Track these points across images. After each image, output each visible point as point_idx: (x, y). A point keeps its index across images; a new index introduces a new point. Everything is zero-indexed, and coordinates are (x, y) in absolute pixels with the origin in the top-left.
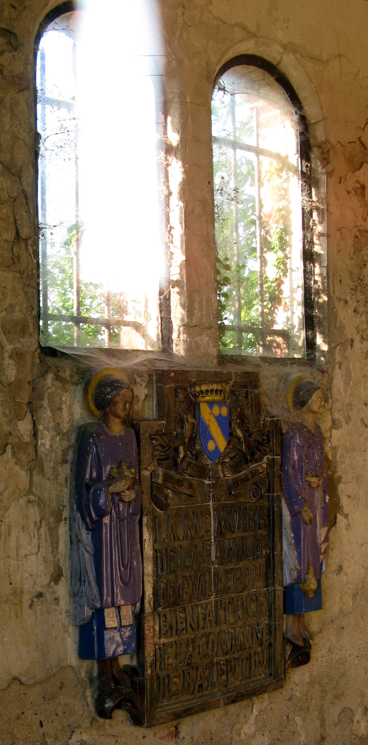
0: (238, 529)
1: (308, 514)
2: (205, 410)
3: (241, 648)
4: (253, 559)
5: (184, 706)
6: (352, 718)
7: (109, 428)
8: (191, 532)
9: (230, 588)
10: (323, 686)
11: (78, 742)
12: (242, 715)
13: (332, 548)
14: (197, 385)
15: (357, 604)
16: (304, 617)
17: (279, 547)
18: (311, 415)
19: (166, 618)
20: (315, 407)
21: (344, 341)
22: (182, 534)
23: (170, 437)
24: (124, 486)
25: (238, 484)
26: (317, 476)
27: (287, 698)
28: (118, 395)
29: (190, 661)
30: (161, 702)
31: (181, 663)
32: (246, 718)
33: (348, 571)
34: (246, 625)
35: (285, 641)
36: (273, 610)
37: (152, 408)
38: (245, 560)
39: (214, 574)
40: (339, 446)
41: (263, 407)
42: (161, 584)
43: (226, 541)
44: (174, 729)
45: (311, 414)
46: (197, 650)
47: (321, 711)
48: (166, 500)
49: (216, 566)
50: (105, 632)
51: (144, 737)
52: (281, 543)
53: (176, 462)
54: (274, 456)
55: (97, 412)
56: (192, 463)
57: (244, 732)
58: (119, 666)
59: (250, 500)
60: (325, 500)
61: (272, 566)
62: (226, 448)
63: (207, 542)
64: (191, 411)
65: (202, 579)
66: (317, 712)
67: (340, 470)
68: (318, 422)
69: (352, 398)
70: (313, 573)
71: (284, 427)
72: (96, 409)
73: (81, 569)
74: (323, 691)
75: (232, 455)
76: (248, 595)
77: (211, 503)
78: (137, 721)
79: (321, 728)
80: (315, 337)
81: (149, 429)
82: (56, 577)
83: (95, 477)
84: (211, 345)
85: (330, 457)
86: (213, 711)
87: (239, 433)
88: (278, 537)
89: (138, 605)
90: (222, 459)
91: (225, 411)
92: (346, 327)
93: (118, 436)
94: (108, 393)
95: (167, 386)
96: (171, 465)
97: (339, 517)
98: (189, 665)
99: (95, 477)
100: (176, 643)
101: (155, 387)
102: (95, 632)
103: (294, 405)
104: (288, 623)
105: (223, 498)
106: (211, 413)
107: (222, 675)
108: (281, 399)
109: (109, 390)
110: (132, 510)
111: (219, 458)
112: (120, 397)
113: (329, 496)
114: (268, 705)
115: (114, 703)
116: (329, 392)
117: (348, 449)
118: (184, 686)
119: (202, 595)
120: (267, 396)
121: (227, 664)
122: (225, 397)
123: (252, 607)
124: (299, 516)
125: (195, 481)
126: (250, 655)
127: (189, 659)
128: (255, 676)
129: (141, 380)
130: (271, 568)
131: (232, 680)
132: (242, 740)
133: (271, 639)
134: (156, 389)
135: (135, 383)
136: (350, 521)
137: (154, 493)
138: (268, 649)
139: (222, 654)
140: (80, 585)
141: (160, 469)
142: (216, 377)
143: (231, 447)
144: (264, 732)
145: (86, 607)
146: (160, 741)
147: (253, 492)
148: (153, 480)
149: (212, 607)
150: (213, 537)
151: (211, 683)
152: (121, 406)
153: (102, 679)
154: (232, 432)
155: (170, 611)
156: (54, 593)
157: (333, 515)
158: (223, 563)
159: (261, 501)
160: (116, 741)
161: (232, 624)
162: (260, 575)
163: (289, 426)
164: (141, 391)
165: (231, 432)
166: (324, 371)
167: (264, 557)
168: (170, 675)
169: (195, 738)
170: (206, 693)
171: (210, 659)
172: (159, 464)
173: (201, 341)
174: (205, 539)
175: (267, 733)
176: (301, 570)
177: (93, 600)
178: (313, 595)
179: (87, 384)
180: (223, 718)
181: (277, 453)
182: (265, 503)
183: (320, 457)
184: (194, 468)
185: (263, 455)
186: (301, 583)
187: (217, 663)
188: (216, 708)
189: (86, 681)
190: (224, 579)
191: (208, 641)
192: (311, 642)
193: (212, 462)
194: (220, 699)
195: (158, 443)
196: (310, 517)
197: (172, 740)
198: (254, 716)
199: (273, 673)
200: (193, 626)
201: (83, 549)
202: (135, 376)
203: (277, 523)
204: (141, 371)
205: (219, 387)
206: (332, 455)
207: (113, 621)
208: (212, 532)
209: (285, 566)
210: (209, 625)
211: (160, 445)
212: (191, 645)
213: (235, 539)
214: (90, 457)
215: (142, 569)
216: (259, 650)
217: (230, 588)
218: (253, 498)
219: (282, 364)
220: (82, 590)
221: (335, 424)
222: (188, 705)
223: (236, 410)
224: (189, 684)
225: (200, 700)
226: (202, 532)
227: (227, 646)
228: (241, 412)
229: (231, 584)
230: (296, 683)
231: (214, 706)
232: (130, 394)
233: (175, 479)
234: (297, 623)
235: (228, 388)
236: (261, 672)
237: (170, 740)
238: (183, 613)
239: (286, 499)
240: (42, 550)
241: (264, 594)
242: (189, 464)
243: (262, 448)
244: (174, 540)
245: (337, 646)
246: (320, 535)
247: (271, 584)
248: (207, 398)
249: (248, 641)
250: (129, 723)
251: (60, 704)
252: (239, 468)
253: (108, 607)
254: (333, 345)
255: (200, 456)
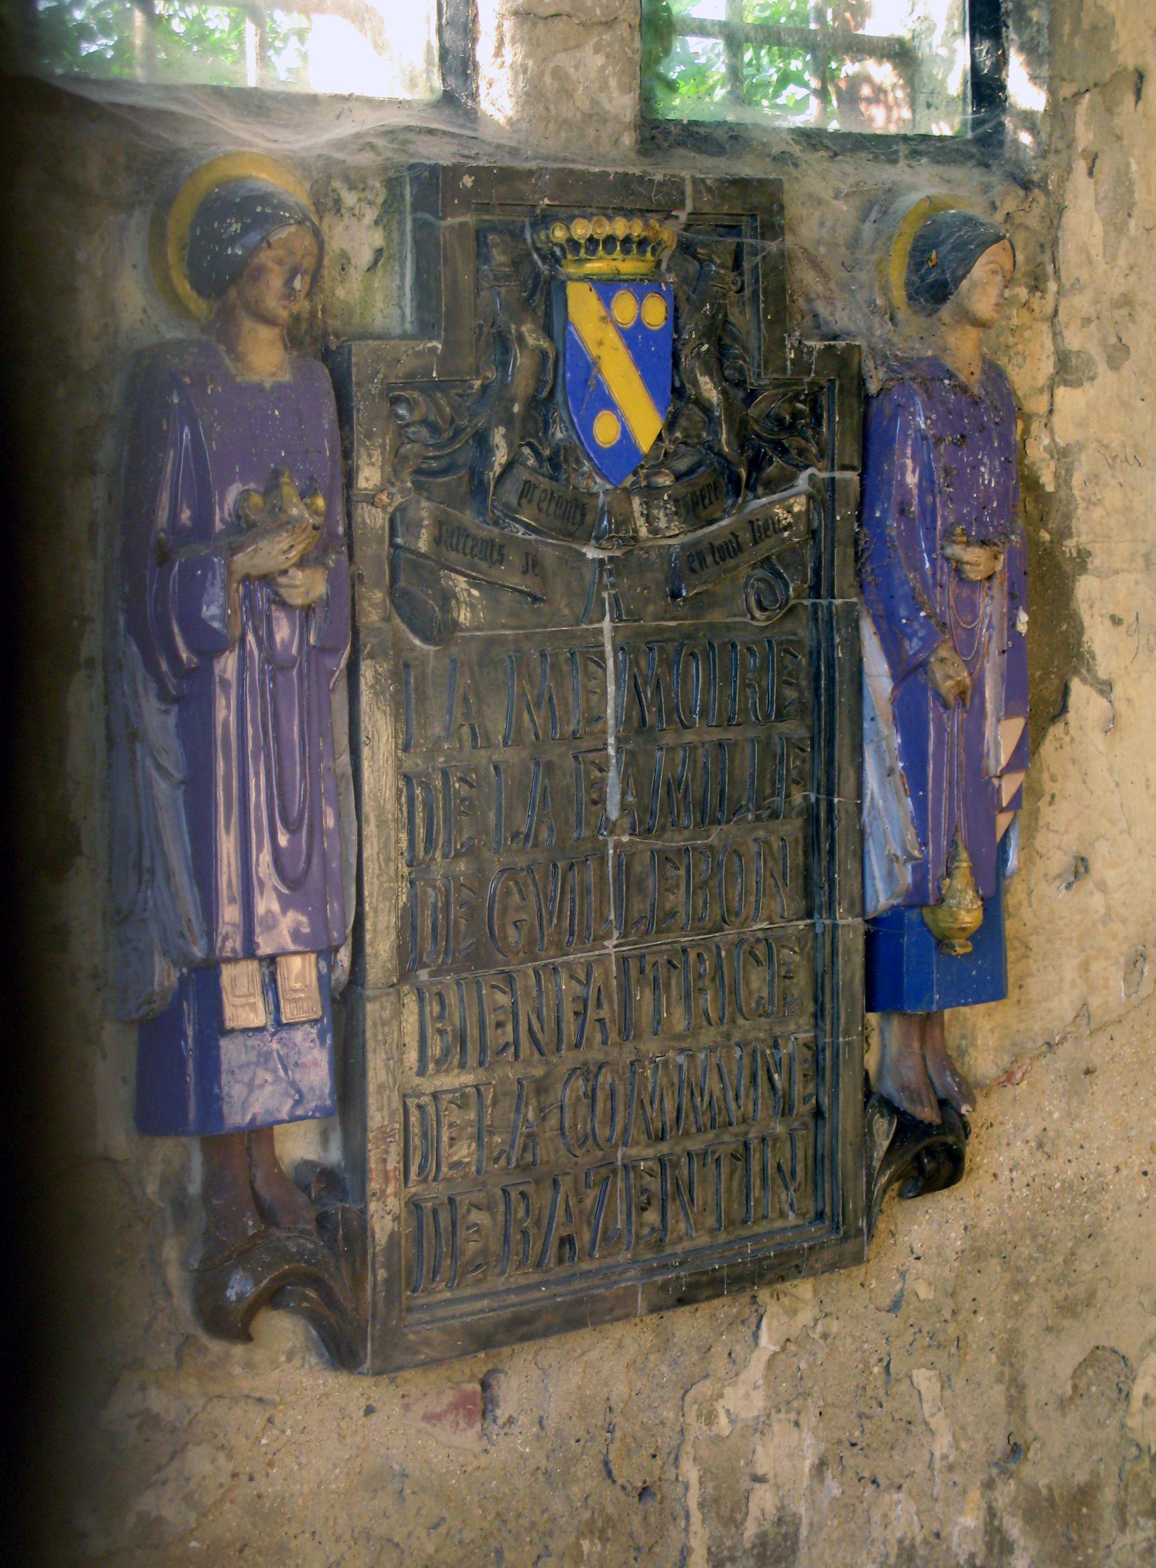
0: (704, 713)
1: (951, 672)
2: (583, 306)
3: (713, 1119)
4: (758, 818)
5: (506, 1307)
6: (1124, 1387)
7: (239, 358)
8: (533, 721)
9: (673, 914)
10: (1019, 1269)
12: (719, 1350)
13: (1053, 796)
14: (557, 219)
15: (1144, 991)
16: (942, 1024)
17: (852, 781)
18: (973, 333)
19: (442, 1004)
20: (983, 305)
21: (1108, 76)
22: (502, 726)
23: (460, 396)
24: (284, 552)
25: (702, 562)
26: (984, 543)
27: (887, 1302)
28: (264, 245)
29: (529, 1158)
30: (430, 1292)
31: (496, 1160)
32: (734, 1362)
33: (1111, 876)
34: (732, 1042)
35: (873, 1101)
36: (828, 997)
37: (401, 297)
38: (728, 822)
39: (618, 865)
40: (1081, 446)
41: (801, 303)
42: (425, 893)
43: (658, 754)
44: (478, 1388)
45: (968, 327)
46: (553, 1121)
47: (1010, 1354)
48: (445, 607)
49: (625, 839)
50: (224, 1043)
51: (369, 1411)
52: (860, 768)
53: (481, 481)
54: (832, 470)
55: (198, 305)
56: (535, 487)
57: (728, 1412)
58: (275, 1162)
59: (748, 619)
60: (1014, 625)
61: (825, 846)
62: (660, 437)
63: (591, 756)
64: (534, 310)
65: (575, 876)
66: (993, 1357)
67: (1084, 528)
68: (1002, 361)
69: (1132, 278)
70: (967, 872)
71: (873, 373)
72: (195, 295)
73: (140, 832)
74: (1017, 1286)
75: (682, 465)
76: (741, 942)
77: (607, 624)
78: (341, 1350)
79: (1009, 1414)
80: (1001, 63)
81: (382, 367)
83: (188, 523)
84: (613, 82)
85: (1048, 482)
86: (618, 1330)
87: (709, 389)
88: (846, 750)
89: (344, 957)
90: (647, 476)
91: (655, 313)
92: (1118, 25)
93: (268, 385)
94: (234, 239)
95: (449, 221)
96: (464, 489)
97: (1079, 690)
98: (524, 1168)
99: (188, 523)
100: (478, 1091)
101: (409, 226)
102: (190, 1040)
103: (910, 298)
104: (883, 1046)
105: (651, 608)
106: (608, 319)
107: (644, 1209)
108: (863, 276)
109: (236, 227)
110: (318, 637)
111: (635, 473)
112: (272, 253)
113: (1027, 612)
114: (816, 1321)
115: (257, 1282)
116: (1047, 257)
117: (1114, 458)
118: (506, 1240)
119: (572, 934)
120: (815, 264)
121: (663, 1173)
122: (658, 264)
123: (755, 985)
124: (921, 678)
125: (550, 550)
126: (746, 1145)
127: (525, 1148)
128: (765, 1217)
129: (360, 200)
130: (824, 855)
131: (682, 1226)
132: (718, 1436)
133: (821, 1095)
134: (414, 231)
135: (339, 210)
136: (1121, 706)
137: (402, 583)
138: (812, 1130)
139: (643, 1138)
140: (140, 883)
141: (424, 504)
142: (625, 195)
143: (678, 434)
144: (799, 1413)
145: (157, 959)
146: (423, 1425)
147: (758, 593)
148: (399, 541)
149: (607, 973)
150: (611, 740)
151: (605, 1233)
152: (276, 281)
153: (215, 1202)
154: (683, 385)
155: (458, 984)
157: (1056, 682)
158: (649, 831)
159: (788, 625)
160: (270, 1420)
161: (681, 1037)
162: (784, 874)
163: (890, 369)
164: (358, 236)
165: (677, 384)
166: (1032, 182)
167: (799, 814)
168: (458, 1199)
169: (551, 1423)
170: (585, 1266)
171: (600, 1154)
172: (418, 486)
173: (576, 67)
174: (585, 745)
175: (810, 1419)
176: (926, 861)
177: (182, 935)
178: (969, 949)
179: (165, 205)
180: (652, 1357)
181: (847, 462)
182: (804, 632)
183: (998, 476)
184: (544, 505)
185: (797, 466)
186: (926, 905)
187: (625, 1166)
188: (618, 1319)
189: (162, 1210)
190: (650, 883)
191: (594, 1090)
192: (964, 1109)
193: (609, 487)
194: (631, 1293)
195: (417, 416)
196: (958, 683)
197: (472, 1426)
198: (764, 1358)
199: (828, 1209)
200: (540, 1036)
201: (149, 762)
202: (336, 184)
203: (843, 700)
204: (358, 169)
205: (637, 229)
206: (1056, 475)
207: (253, 1007)
208: (611, 722)
209: (871, 846)
210: (598, 1037)
211: (424, 422)
212: (533, 1102)
213: (693, 748)
214: (172, 454)
215: (355, 838)
216: (779, 1129)
217: (673, 914)
218: (758, 614)
219: (876, 158)
220: (146, 902)
221: (1066, 368)
222: (521, 1304)
223: (698, 309)
224: (524, 1233)
225: (563, 1289)
226: (574, 721)
227: (662, 1110)
228: (714, 316)
229: (676, 900)
230: (918, 1251)
231: (612, 1310)
232: (308, 241)
233: (474, 538)
234: (916, 1045)
235: (668, 234)
236: (786, 1207)
237: (462, 1425)
238: (504, 992)
239: (876, 620)
241: (799, 940)
242: (527, 490)
243: (792, 443)
244: (475, 747)
245: (1068, 1132)
246: (997, 744)
247: (821, 906)
248: (595, 266)
249: (737, 1097)
250: (314, 1360)
252: (705, 508)
253: (233, 960)
254: (1067, 90)
255: (566, 460)
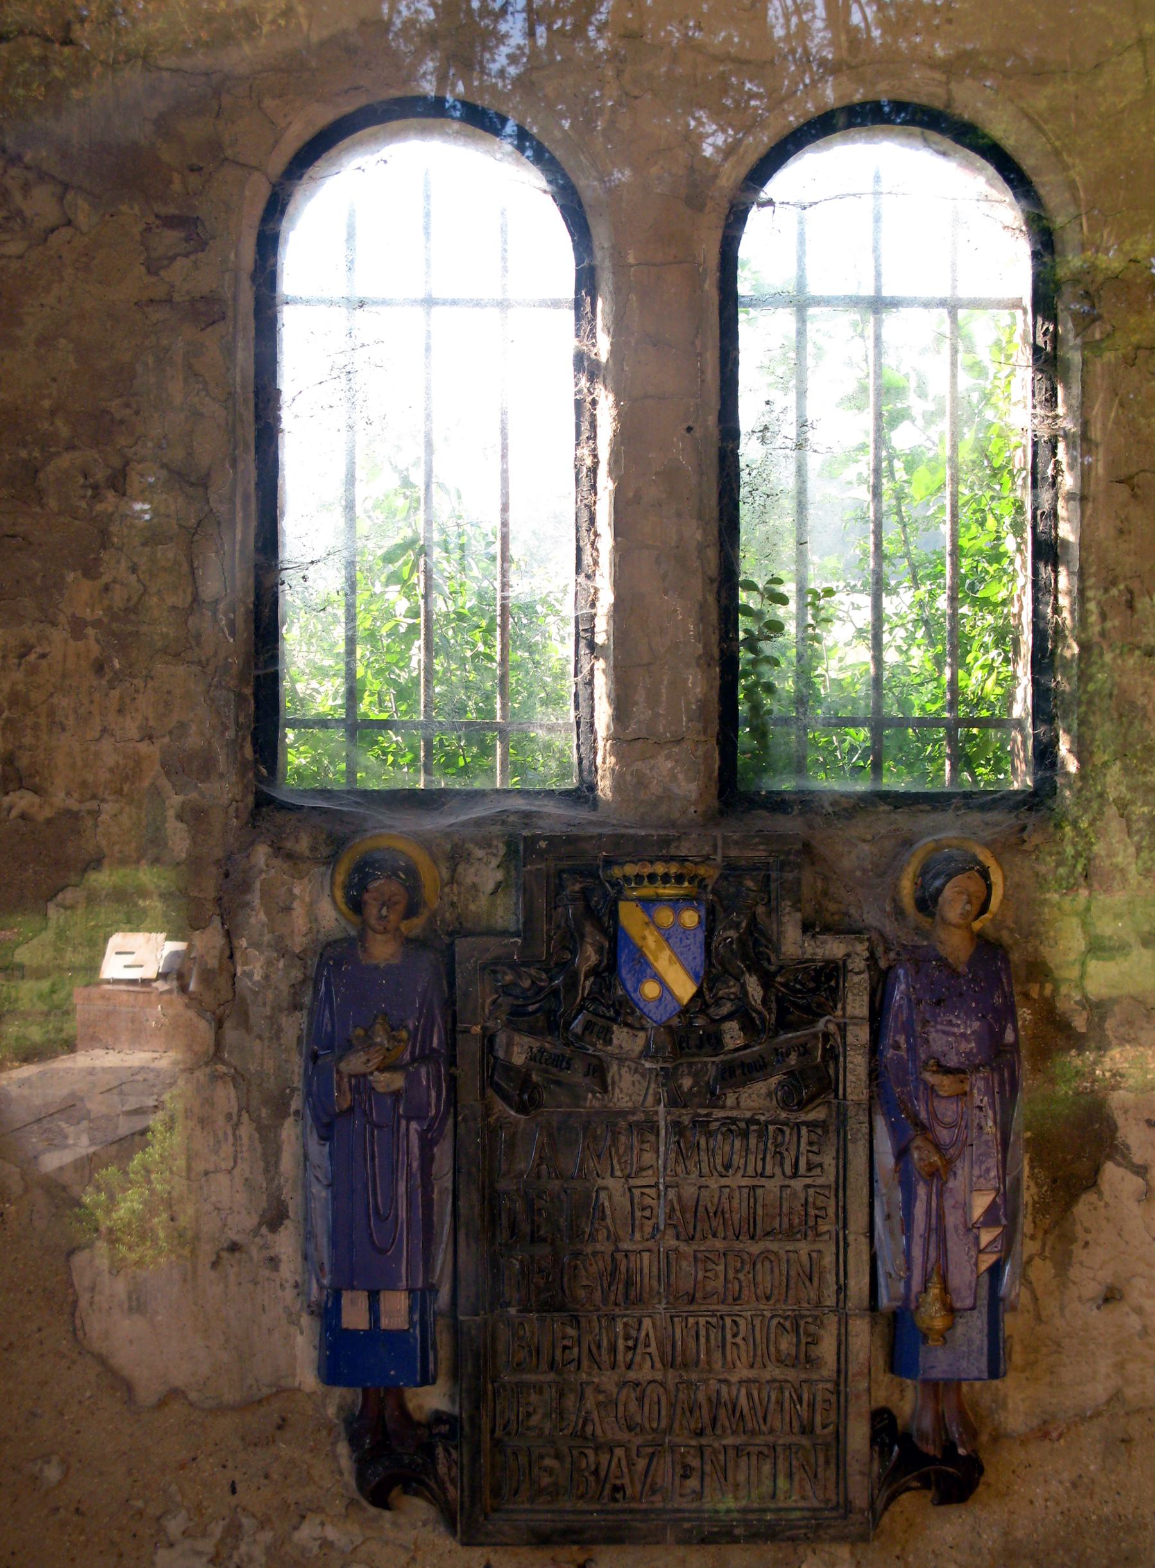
11: (315, 1539)
82: (275, 1218)
156: (265, 1246)
240: (241, 1165)
250: (442, 1529)
251: (277, 1458)
